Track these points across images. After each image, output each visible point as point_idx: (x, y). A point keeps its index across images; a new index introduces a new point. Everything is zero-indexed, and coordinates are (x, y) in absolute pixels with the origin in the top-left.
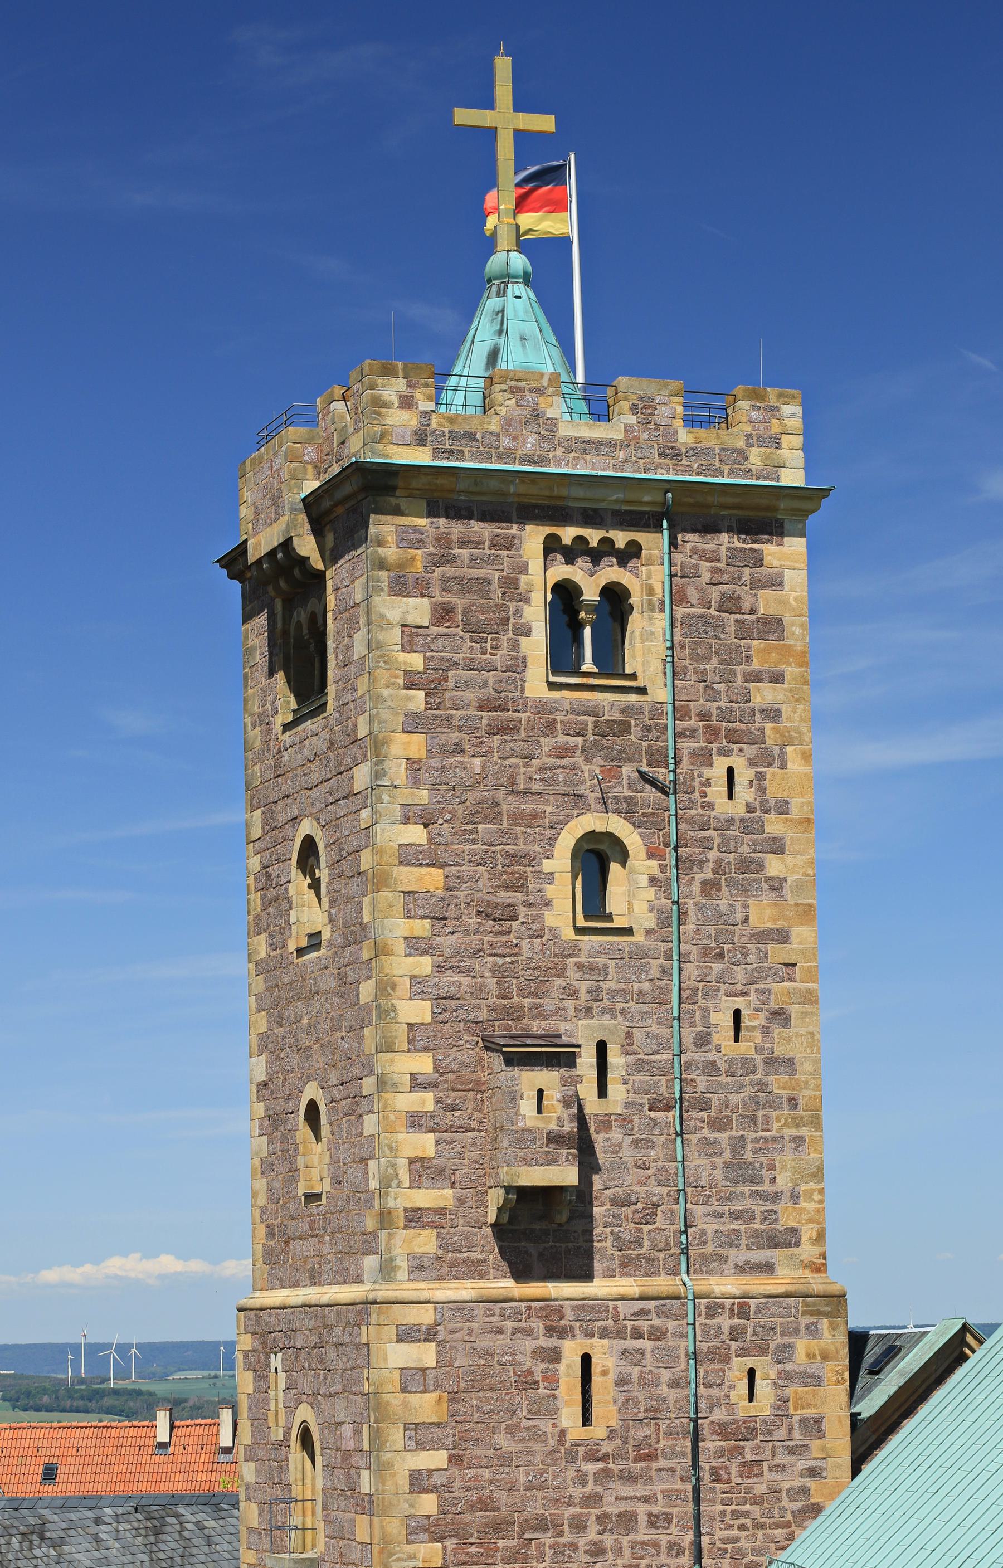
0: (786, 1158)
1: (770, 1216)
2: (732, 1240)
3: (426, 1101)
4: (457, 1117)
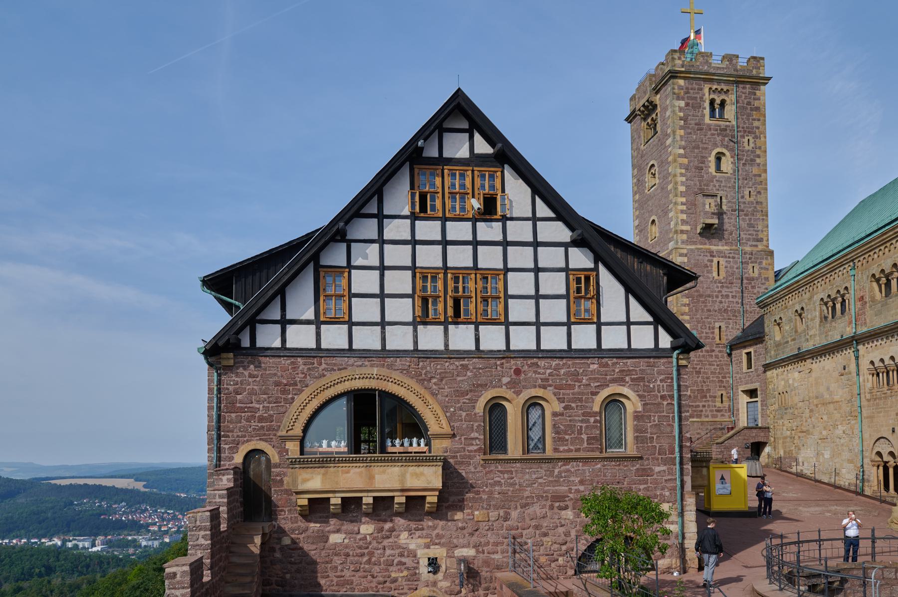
0: (760, 223)
1: (757, 235)
2: (749, 240)
3: (684, 208)
4: (691, 211)
